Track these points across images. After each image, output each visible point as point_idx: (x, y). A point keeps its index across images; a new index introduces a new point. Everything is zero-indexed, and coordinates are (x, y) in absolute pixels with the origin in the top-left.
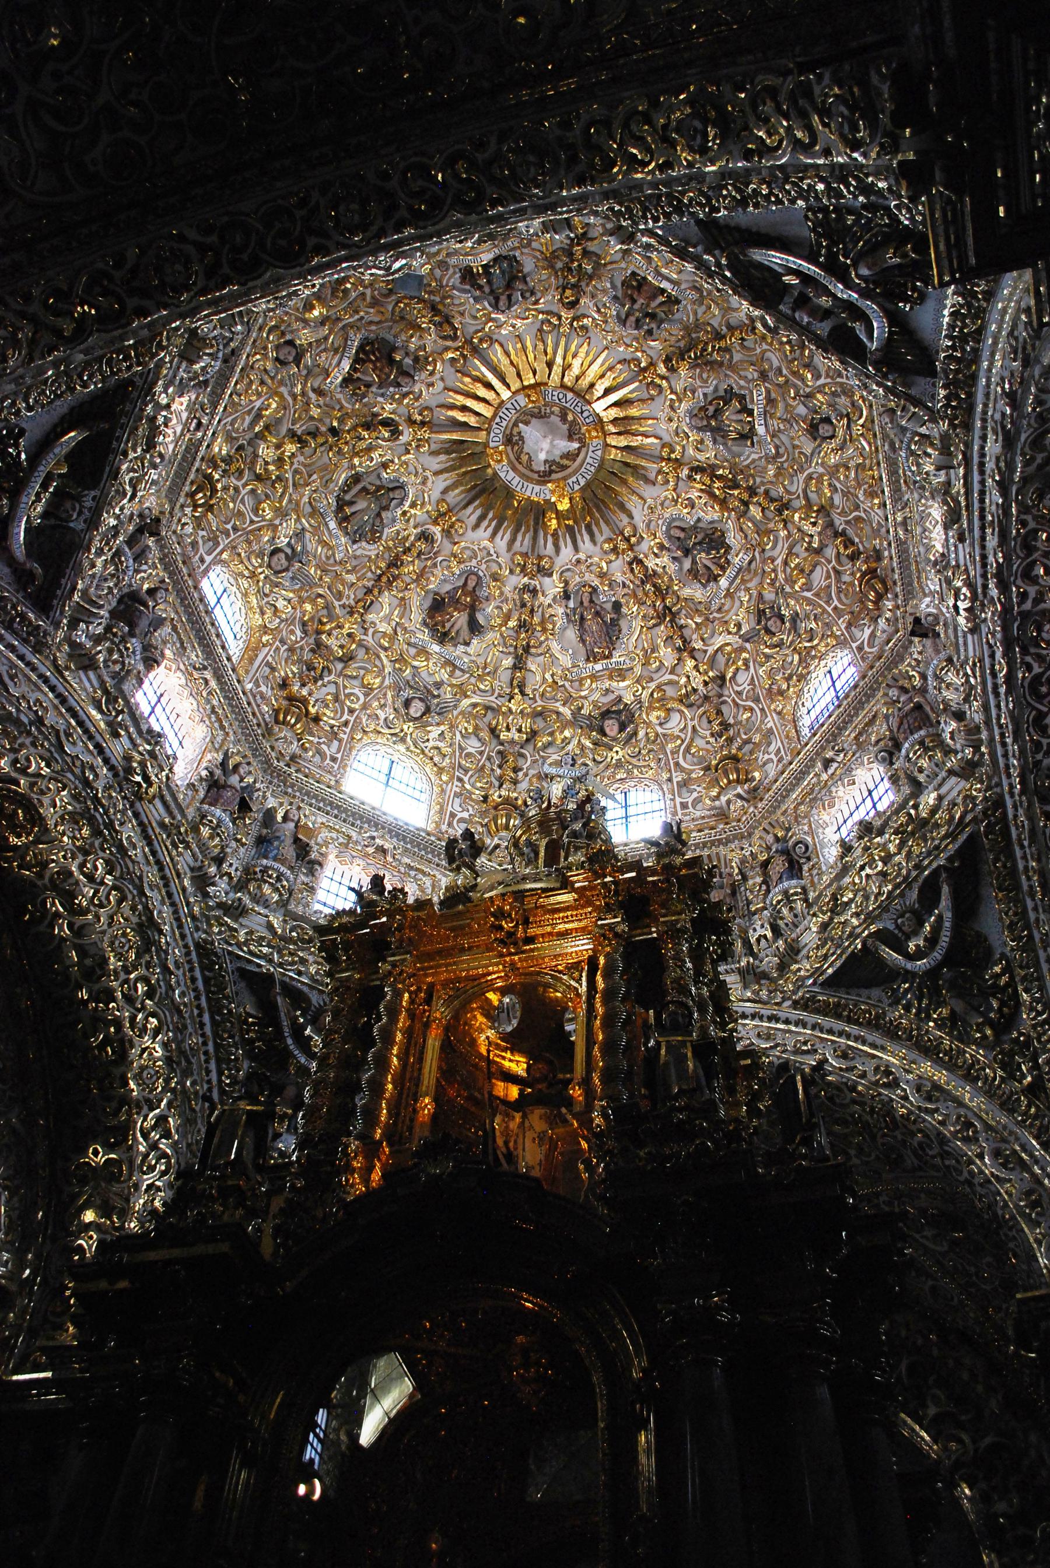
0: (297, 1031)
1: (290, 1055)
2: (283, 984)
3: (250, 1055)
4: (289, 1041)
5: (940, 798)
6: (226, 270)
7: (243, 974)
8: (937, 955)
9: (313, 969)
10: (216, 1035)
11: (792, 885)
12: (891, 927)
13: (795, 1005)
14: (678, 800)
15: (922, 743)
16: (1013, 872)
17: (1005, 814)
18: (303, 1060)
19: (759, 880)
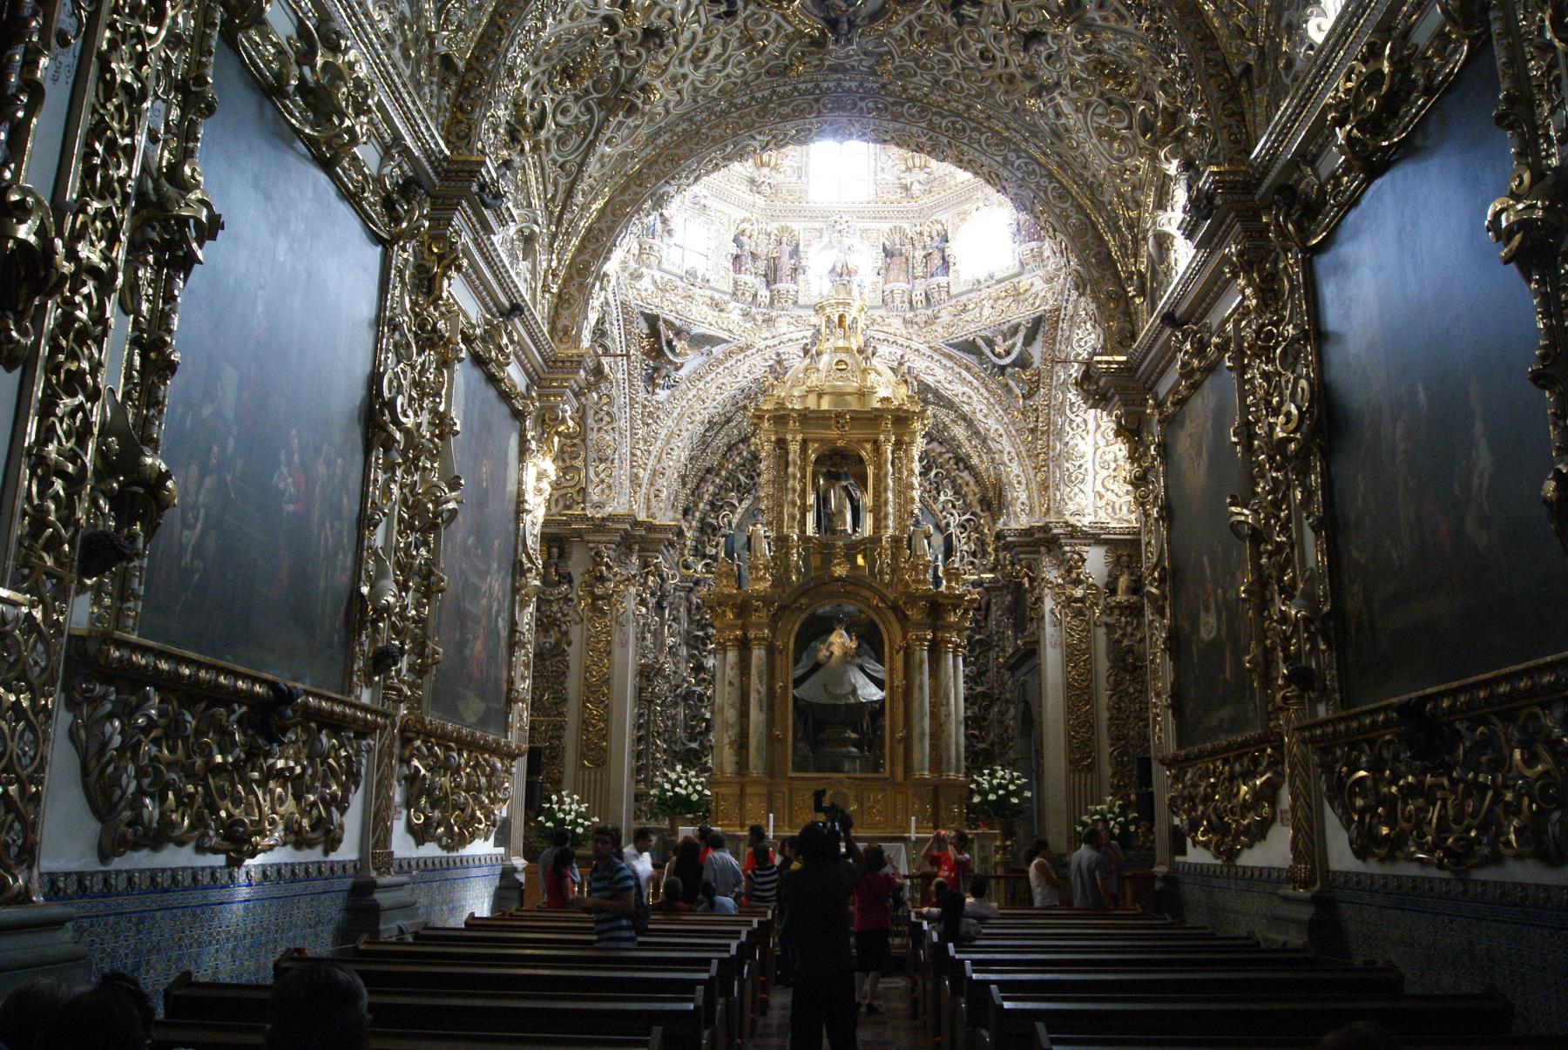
0: (669, 343)
1: (665, 354)
2: (665, 321)
3: (643, 354)
4: (665, 348)
5: (1032, 285)
6: (771, 146)
7: (642, 313)
8: (1008, 360)
9: (679, 307)
10: (627, 346)
11: (942, 280)
12: (990, 335)
13: (930, 348)
14: (879, 164)
15: (1032, 250)
16: (1054, 339)
17: (1058, 317)
18: (671, 357)
19: (923, 253)
